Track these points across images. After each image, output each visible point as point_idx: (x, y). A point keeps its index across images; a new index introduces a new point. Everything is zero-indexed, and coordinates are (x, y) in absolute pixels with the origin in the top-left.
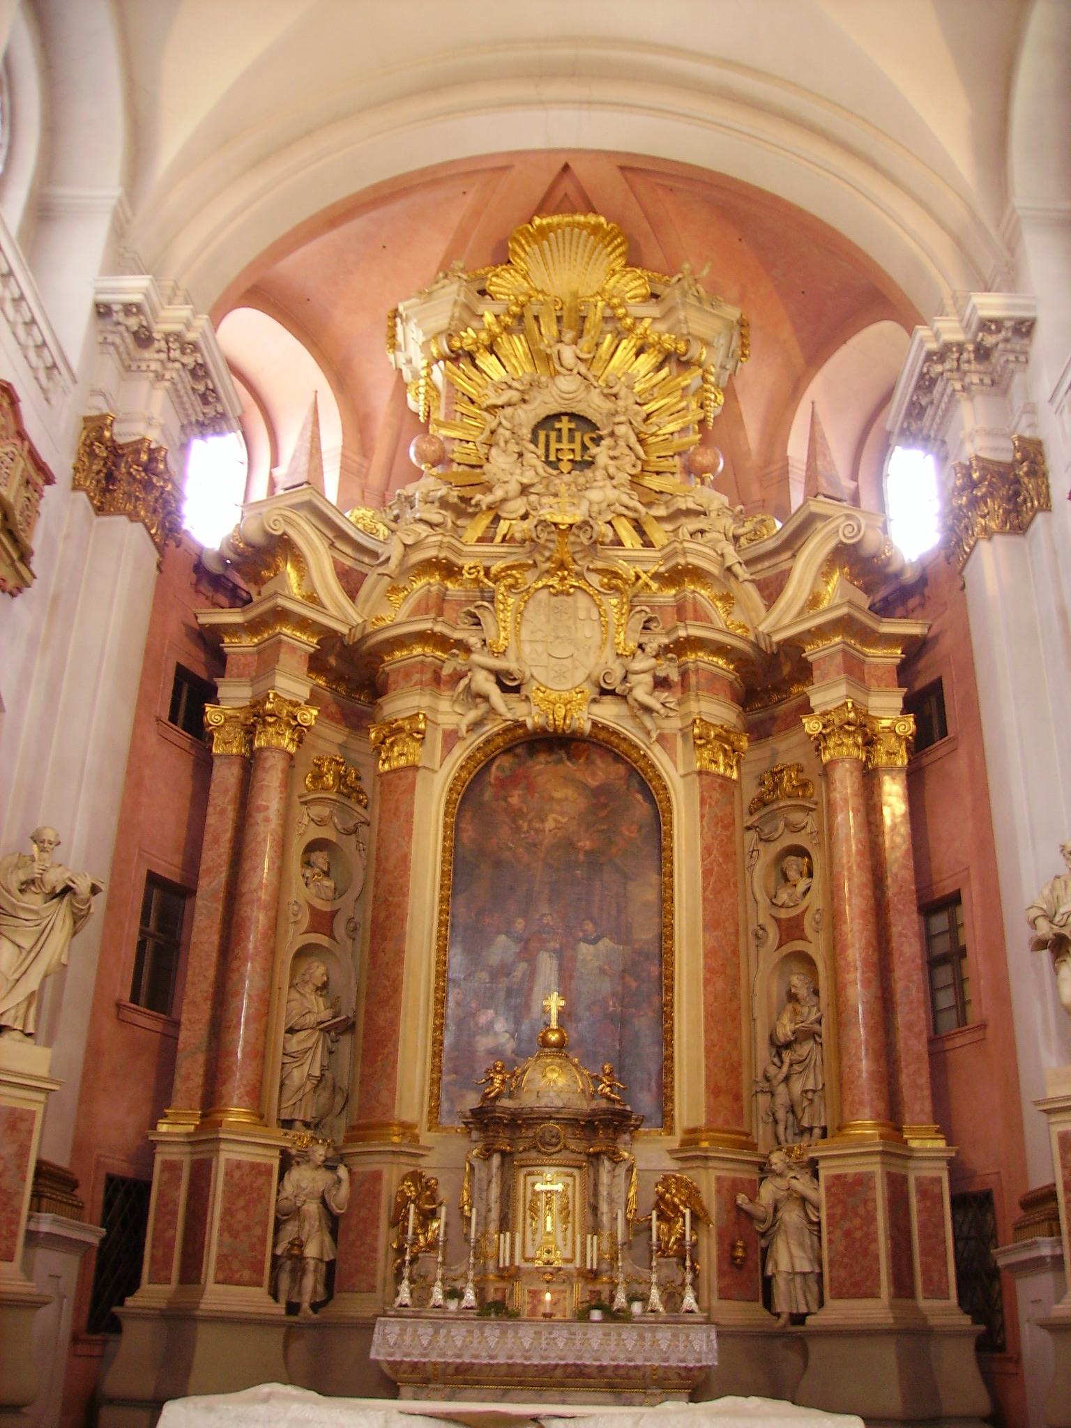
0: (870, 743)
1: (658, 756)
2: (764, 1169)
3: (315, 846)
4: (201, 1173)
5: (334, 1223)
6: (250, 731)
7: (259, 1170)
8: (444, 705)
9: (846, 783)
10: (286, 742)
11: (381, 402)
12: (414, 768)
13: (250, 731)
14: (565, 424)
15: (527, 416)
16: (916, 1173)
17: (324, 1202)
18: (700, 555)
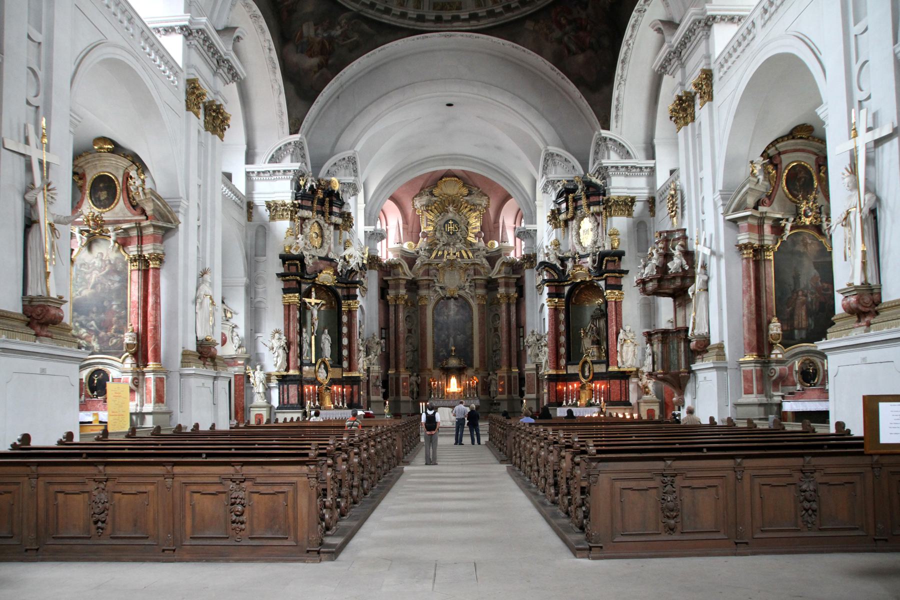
0: (509, 299)
1: (471, 301)
2: (489, 374)
3: (408, 316)
4: (397, 379)
5: (418, 385)
6: (396, 301)
7: (407, 378)
8: (431, 292)
9: (504, 307)
10: (403, 302)
11: (410, 211)
12: (426, 305)
13: (396, 301)
14: (451, 222)
15: (442, 222)
16: (513, 375)
17: (416, 382)
18: (478, 261)
